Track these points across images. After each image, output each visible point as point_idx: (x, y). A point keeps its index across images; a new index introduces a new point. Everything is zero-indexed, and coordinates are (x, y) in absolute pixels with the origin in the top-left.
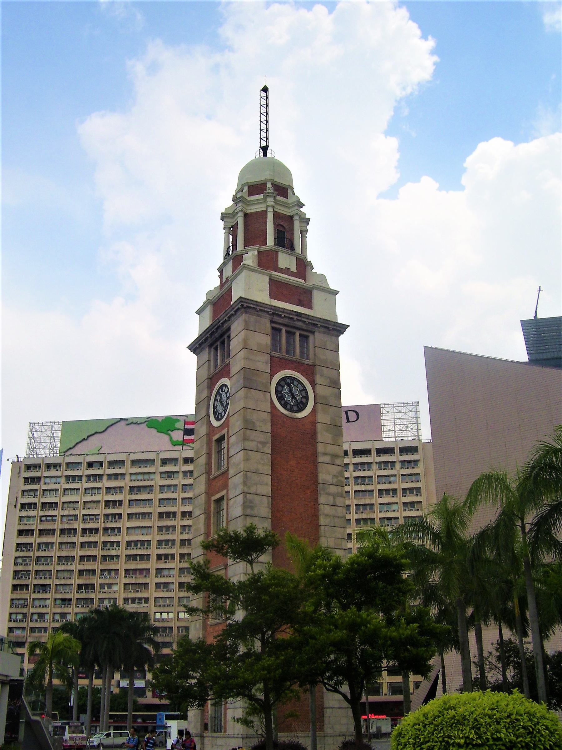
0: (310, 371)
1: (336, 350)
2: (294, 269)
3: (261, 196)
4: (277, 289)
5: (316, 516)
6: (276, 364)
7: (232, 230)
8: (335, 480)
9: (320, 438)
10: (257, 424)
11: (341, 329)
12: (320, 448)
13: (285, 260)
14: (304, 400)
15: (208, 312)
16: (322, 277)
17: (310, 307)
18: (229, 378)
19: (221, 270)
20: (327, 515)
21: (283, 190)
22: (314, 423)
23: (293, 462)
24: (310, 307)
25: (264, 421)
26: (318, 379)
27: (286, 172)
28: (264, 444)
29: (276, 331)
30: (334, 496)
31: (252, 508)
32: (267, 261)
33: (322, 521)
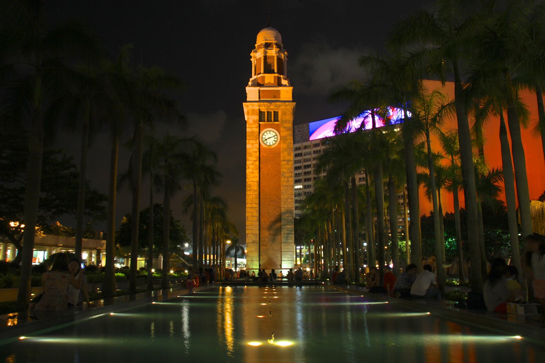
2: (273, 82)
5: (279, 187)
8: (289, 171)
9: (282, 154)
10: (253, 153)
12: (282, 158)
14: (276, 140)
20: (284, 186)
22: (279, 149)
23: (269, 166)
25: (256, 152)
26: (282, 129)
28: (255, 161)
30: (288, 178)
31: (250, 187)
33: (282, 188)
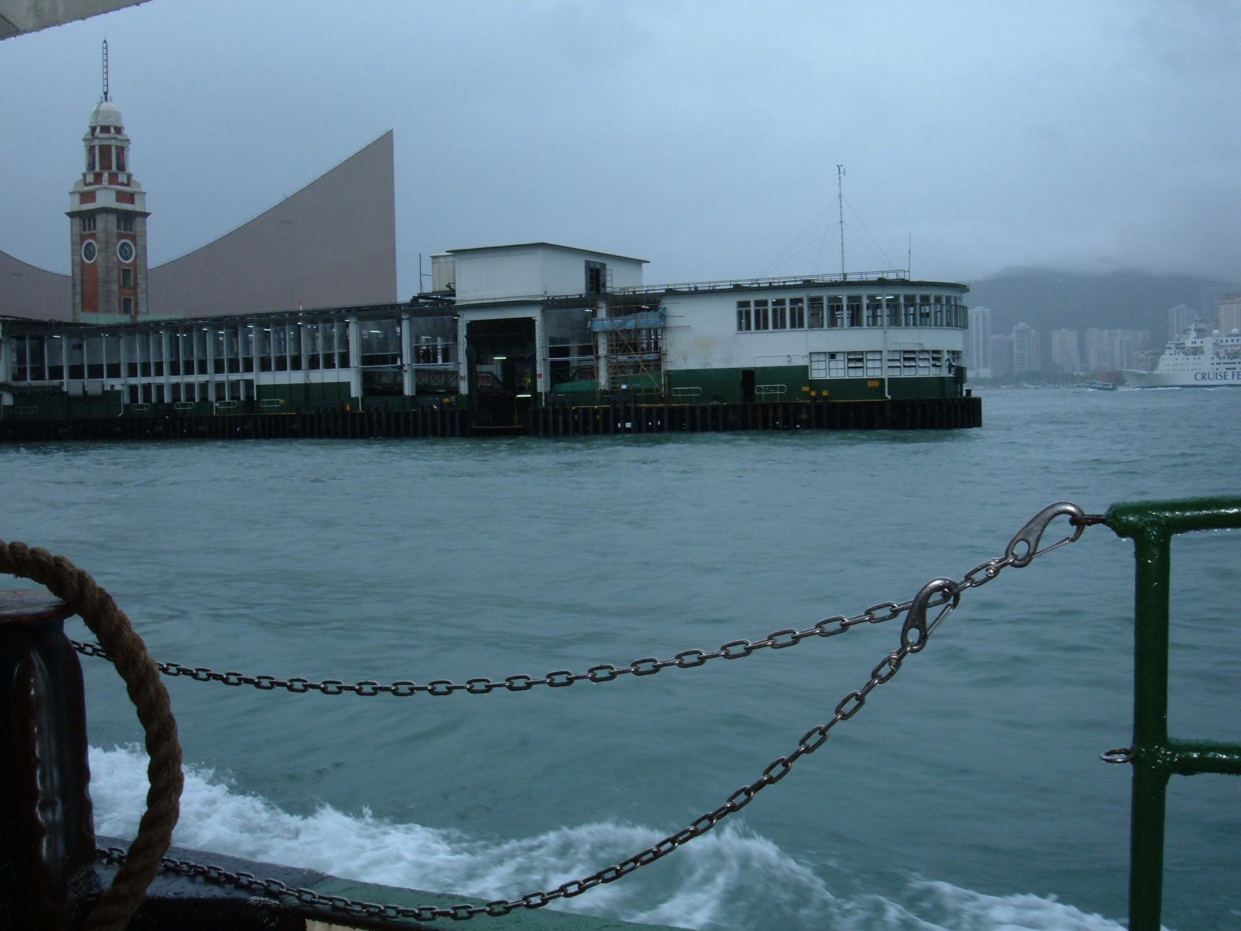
0: (133, 238)
1: (144, 225)
3: (106, 135)
4: (121, 197)
6: (120, 236)
7: (91, 150)
11: (146, 215)
15: (77, 197)
16: (138, 185)
17: (133, 202)
18: (95, 239)
19: (84, 175)
21: (119, 130)
24: (133, 202)
27: (117, 115)
29: (118, 219)
32: (113, 179)
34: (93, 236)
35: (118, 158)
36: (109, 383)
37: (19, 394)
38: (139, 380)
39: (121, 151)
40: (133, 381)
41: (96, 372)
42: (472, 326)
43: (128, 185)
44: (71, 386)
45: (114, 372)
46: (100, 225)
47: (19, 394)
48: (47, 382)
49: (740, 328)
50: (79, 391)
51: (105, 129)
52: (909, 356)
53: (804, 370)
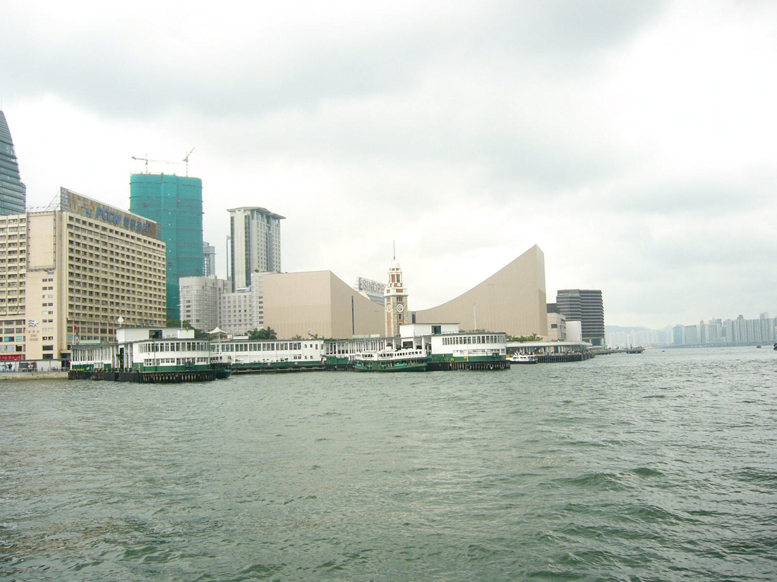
0: (402, 304)
4: (398, 291)
6: (397, 304)
11: (407, 296)
13: (399, 284)
32: (396, 285)
34: (390, 304)
35: (397, 278)
36: (346, 355)
37: (328, 358)
38: (352, 354)
39: (398, 276)
40: (351, 354)
41: (343, 352)
42: (404, 343)
43: (401, 286)
44: (338, 356)
45: (347, 353)
46: (391, 300)
47: (328, 358)
48: (333, 355)
49: (444, 344)
50: (339, 357)
51: (393, 269)
52: (475, 351)
53: (452, 354)
